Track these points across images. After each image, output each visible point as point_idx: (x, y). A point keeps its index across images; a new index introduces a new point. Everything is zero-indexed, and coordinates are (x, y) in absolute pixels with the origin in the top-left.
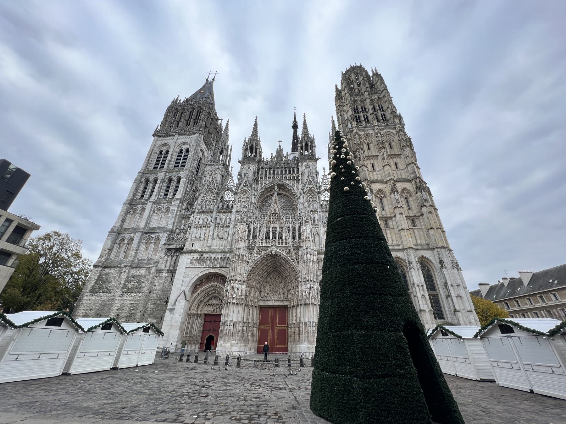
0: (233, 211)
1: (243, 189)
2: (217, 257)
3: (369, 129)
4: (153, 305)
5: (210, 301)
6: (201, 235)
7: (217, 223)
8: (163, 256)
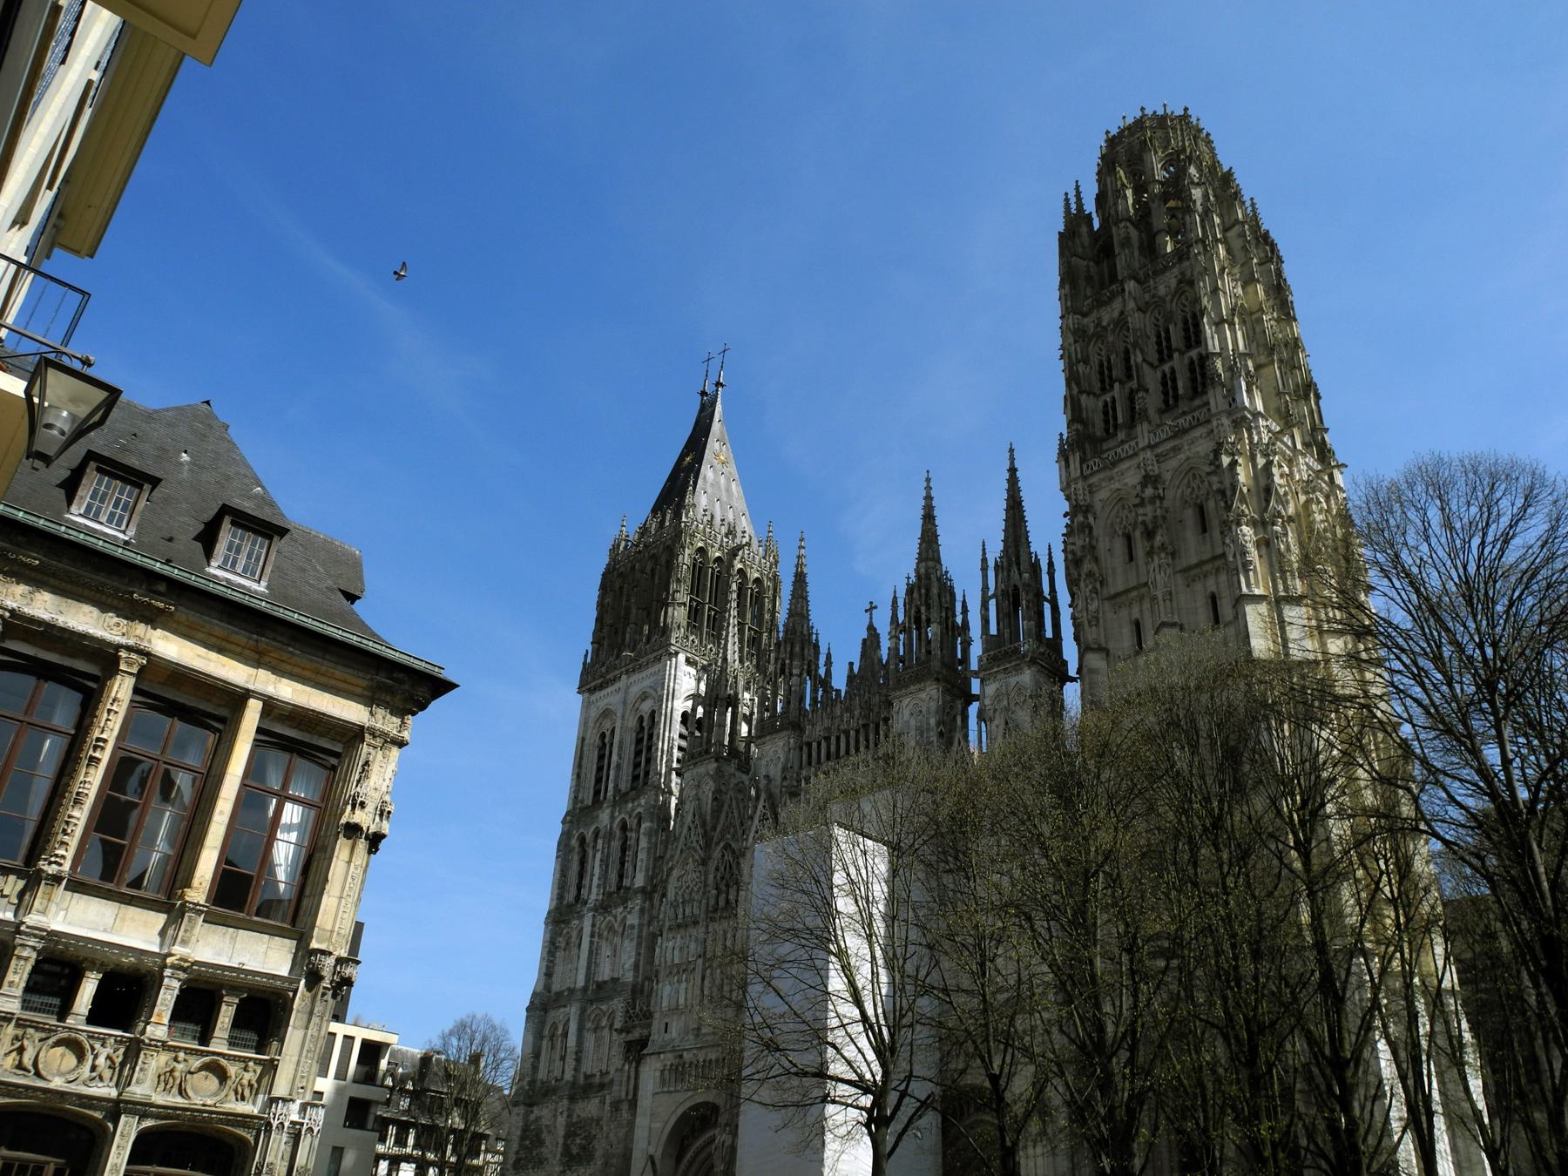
3: (1129, 468)
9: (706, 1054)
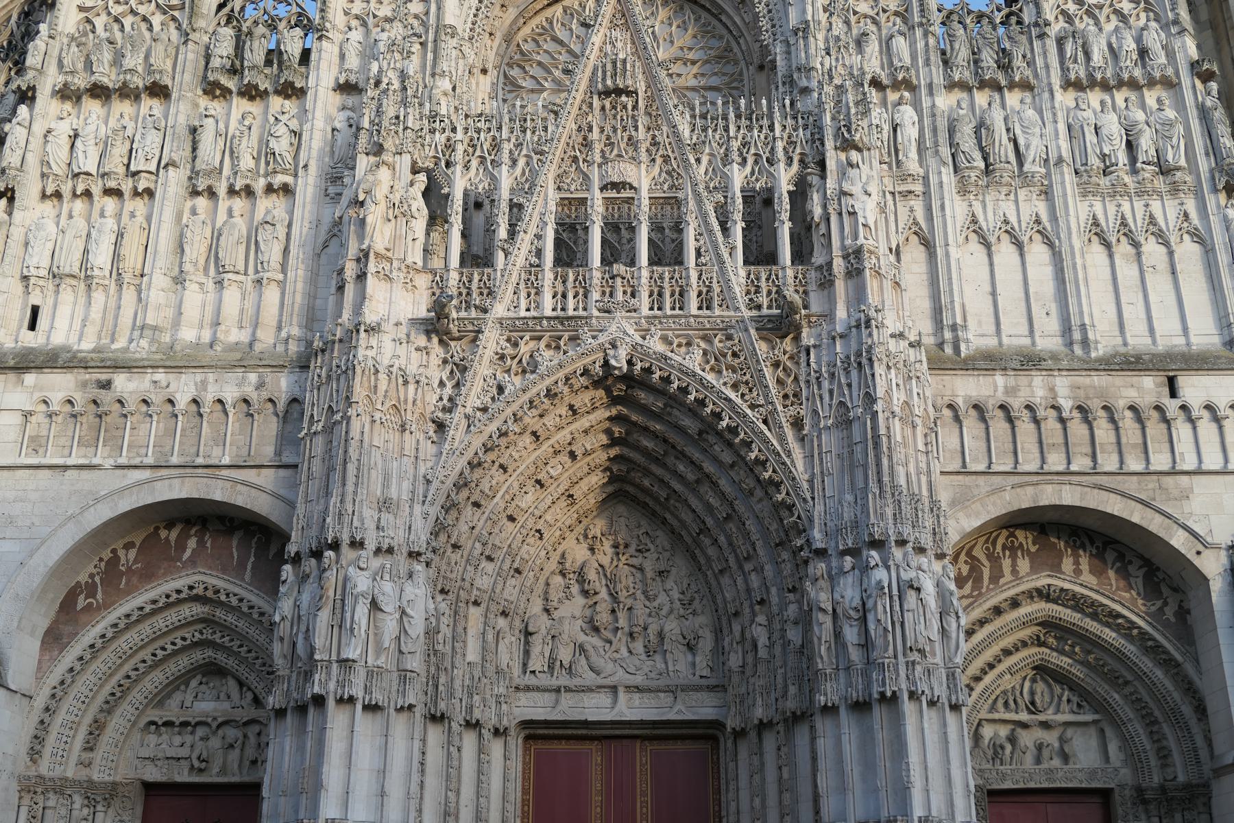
2: (209, 398)
5: (177, 697)
6: (92, 247)
7: (200, 165)
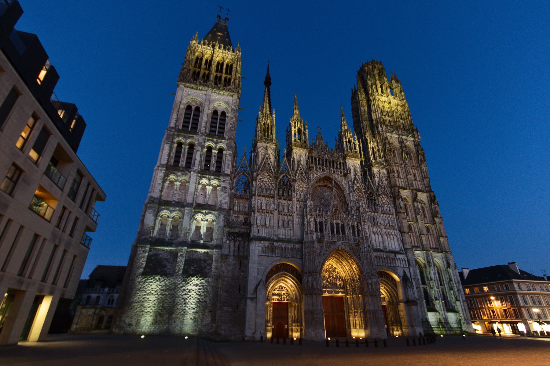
0: (294, 199)
1: (300, 177)
2: (287, 247)
4: (225, 294)
6: (266, 221)
7: (280, 210)
8: (225, 239)
9: (286, 245)
